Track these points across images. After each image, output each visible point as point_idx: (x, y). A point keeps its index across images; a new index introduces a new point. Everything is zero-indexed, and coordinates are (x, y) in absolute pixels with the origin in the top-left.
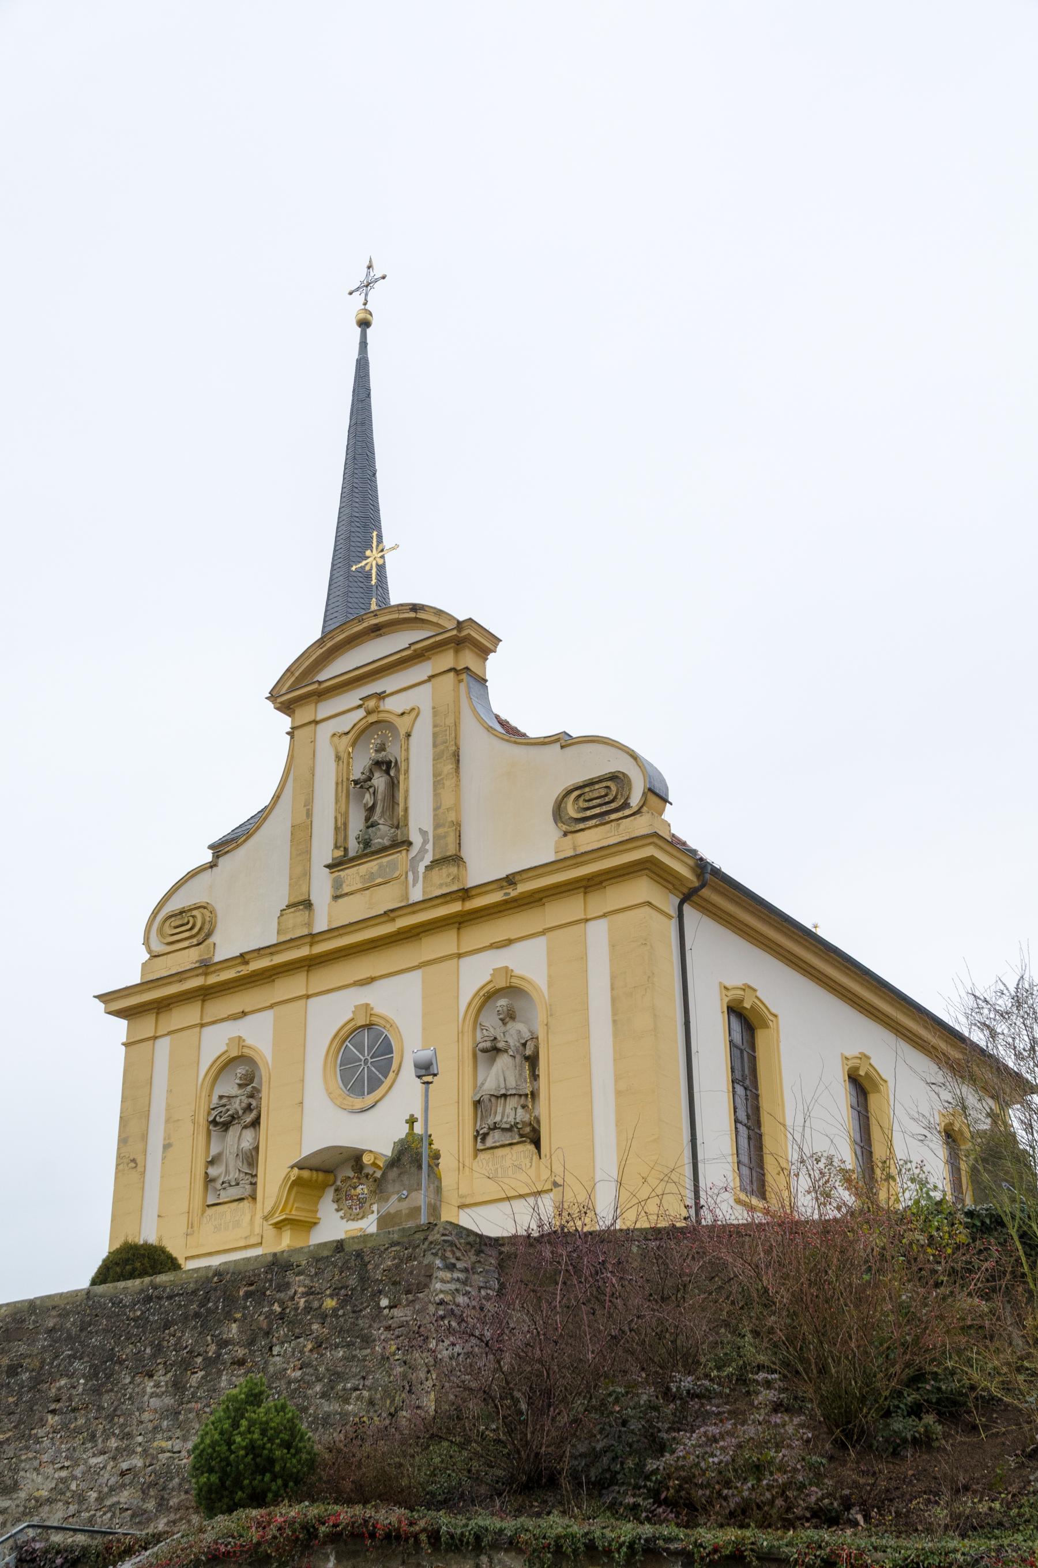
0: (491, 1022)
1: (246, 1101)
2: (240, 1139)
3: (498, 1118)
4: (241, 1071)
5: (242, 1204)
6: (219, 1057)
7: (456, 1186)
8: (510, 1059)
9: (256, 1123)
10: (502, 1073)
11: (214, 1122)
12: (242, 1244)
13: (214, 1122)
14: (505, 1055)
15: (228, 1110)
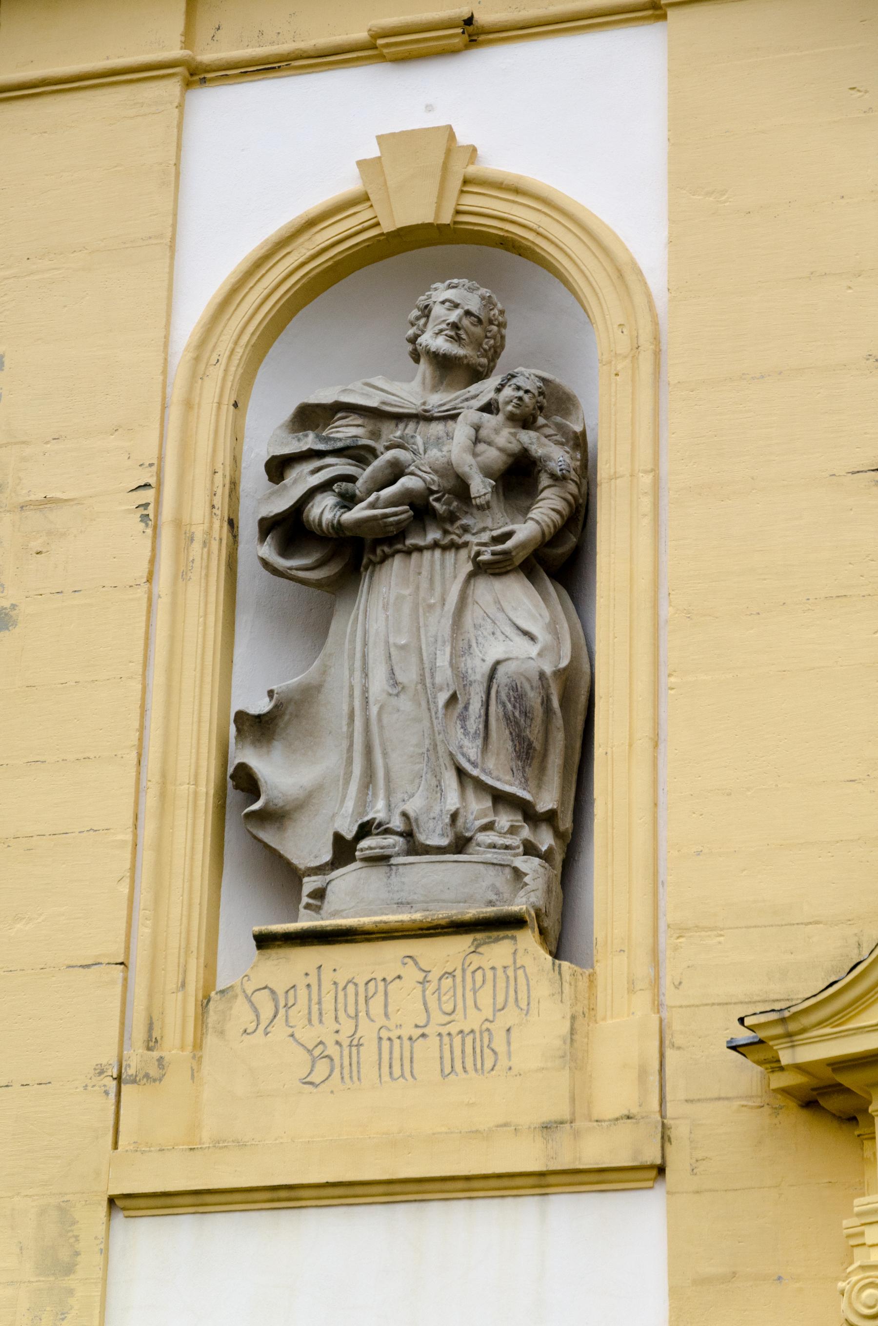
1: (505, 438)
2: (437, 629)
4: (451, 297)
5: (499, 951)
6: (311, 223)
9: (563, 562)
11: (289, 530)
12: (528, 1158)
13: (289, 530)
15: (397, 471)
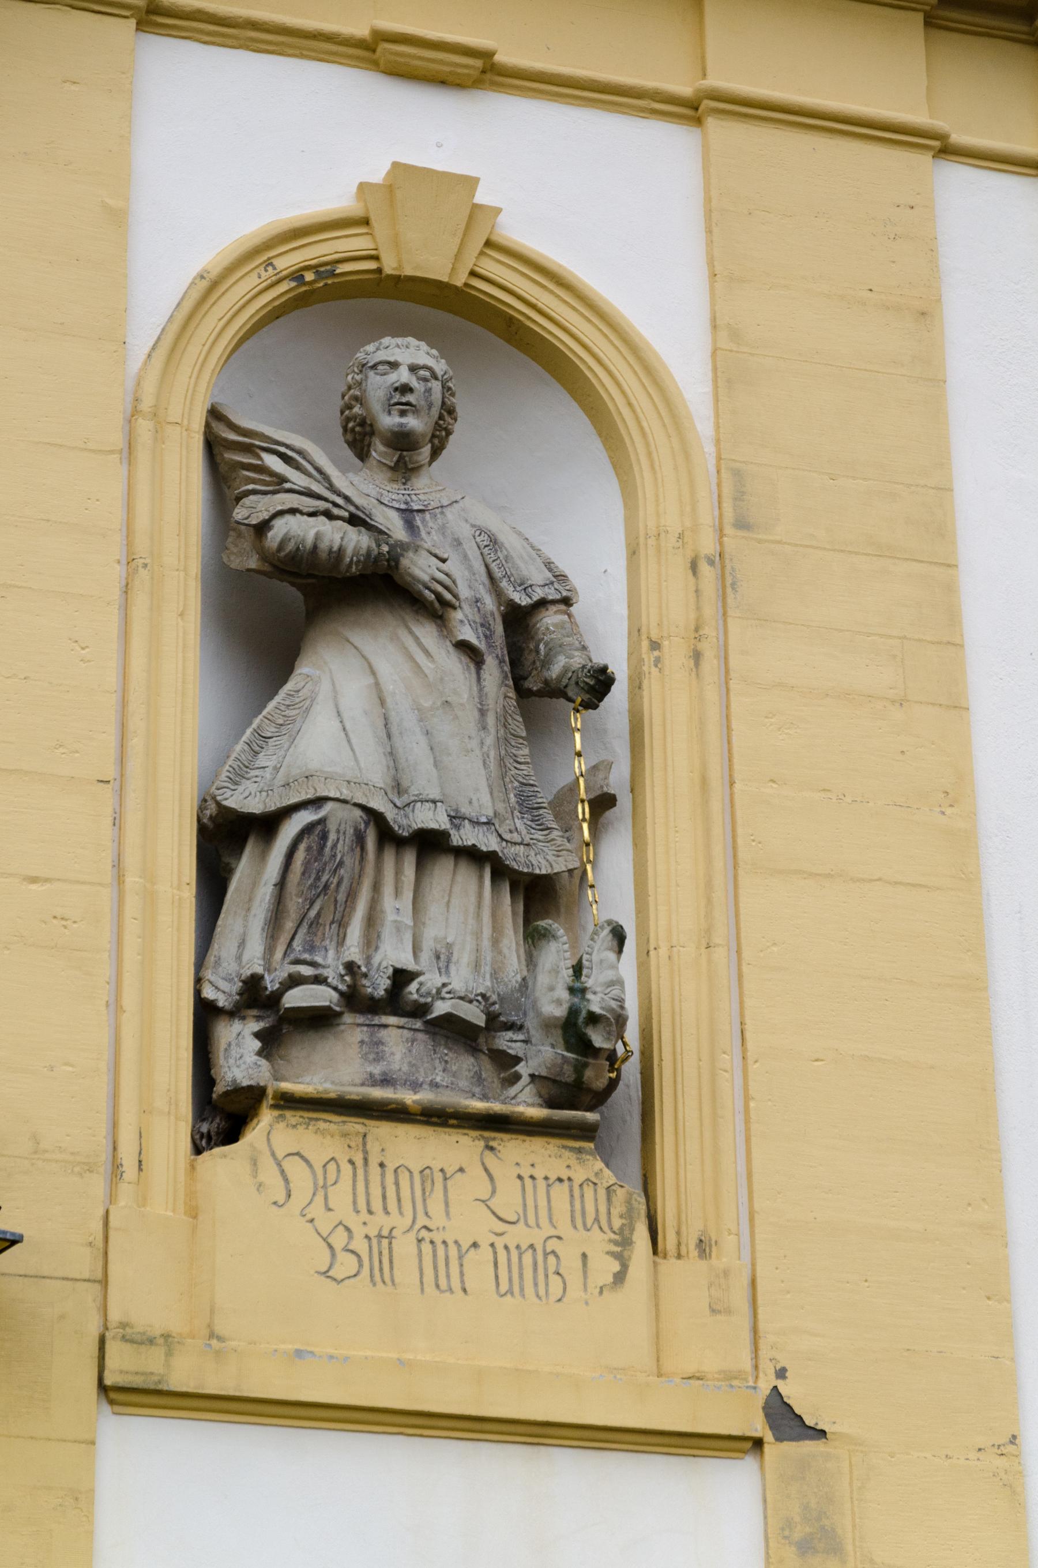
0: (288, 419)
3: (394, 953)
7: (84, 1264)
8: (453, 664)
10: (372, 717)
14: (427, 632)
